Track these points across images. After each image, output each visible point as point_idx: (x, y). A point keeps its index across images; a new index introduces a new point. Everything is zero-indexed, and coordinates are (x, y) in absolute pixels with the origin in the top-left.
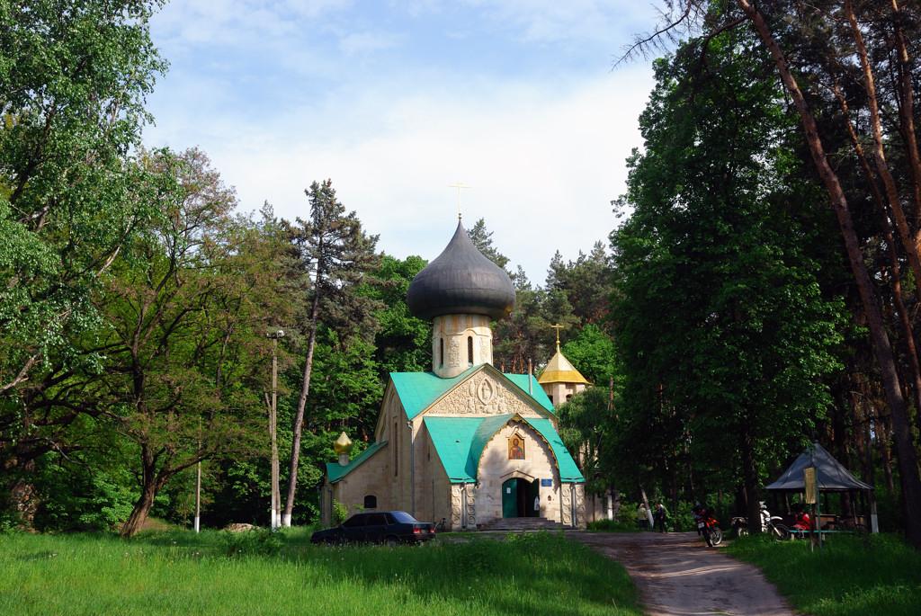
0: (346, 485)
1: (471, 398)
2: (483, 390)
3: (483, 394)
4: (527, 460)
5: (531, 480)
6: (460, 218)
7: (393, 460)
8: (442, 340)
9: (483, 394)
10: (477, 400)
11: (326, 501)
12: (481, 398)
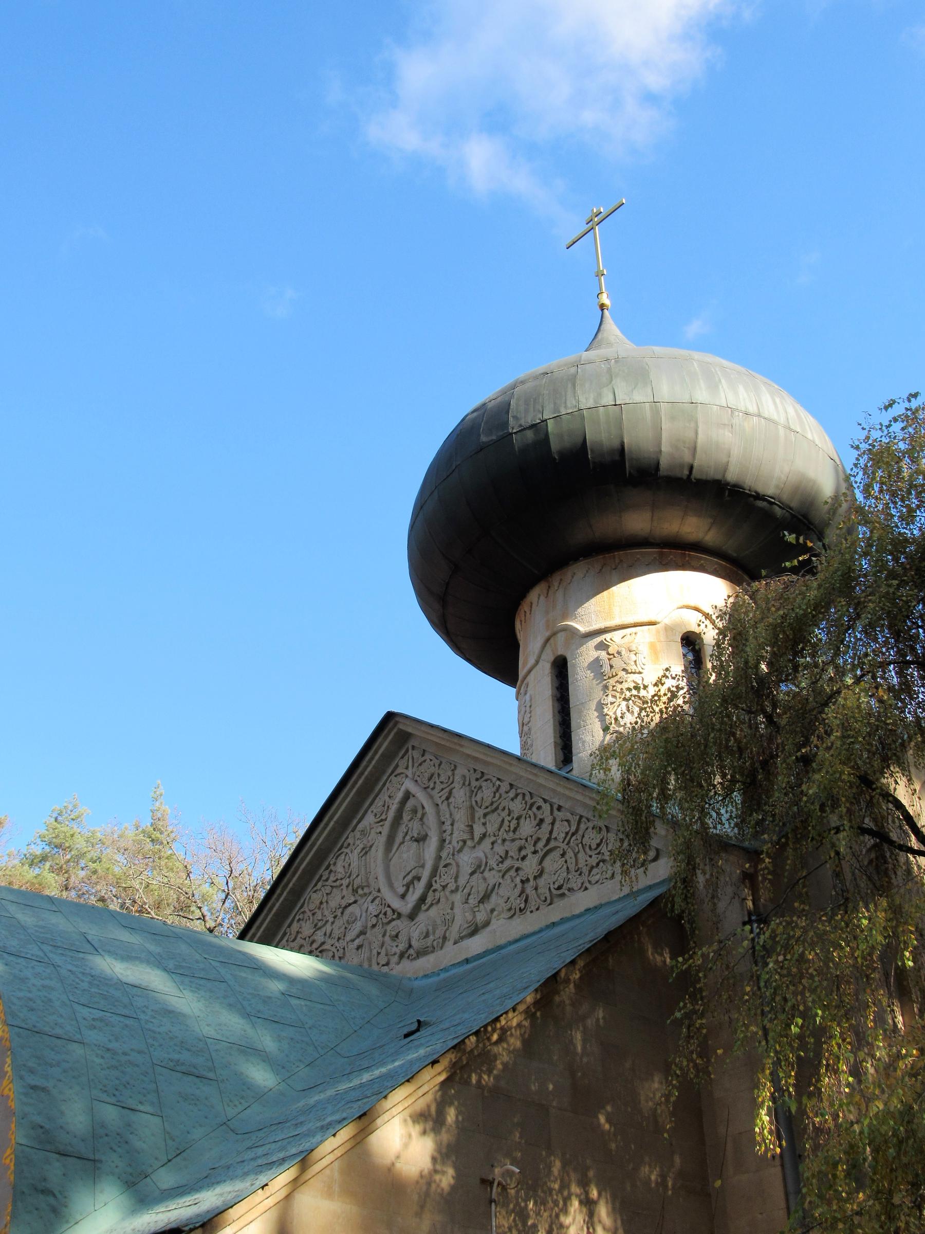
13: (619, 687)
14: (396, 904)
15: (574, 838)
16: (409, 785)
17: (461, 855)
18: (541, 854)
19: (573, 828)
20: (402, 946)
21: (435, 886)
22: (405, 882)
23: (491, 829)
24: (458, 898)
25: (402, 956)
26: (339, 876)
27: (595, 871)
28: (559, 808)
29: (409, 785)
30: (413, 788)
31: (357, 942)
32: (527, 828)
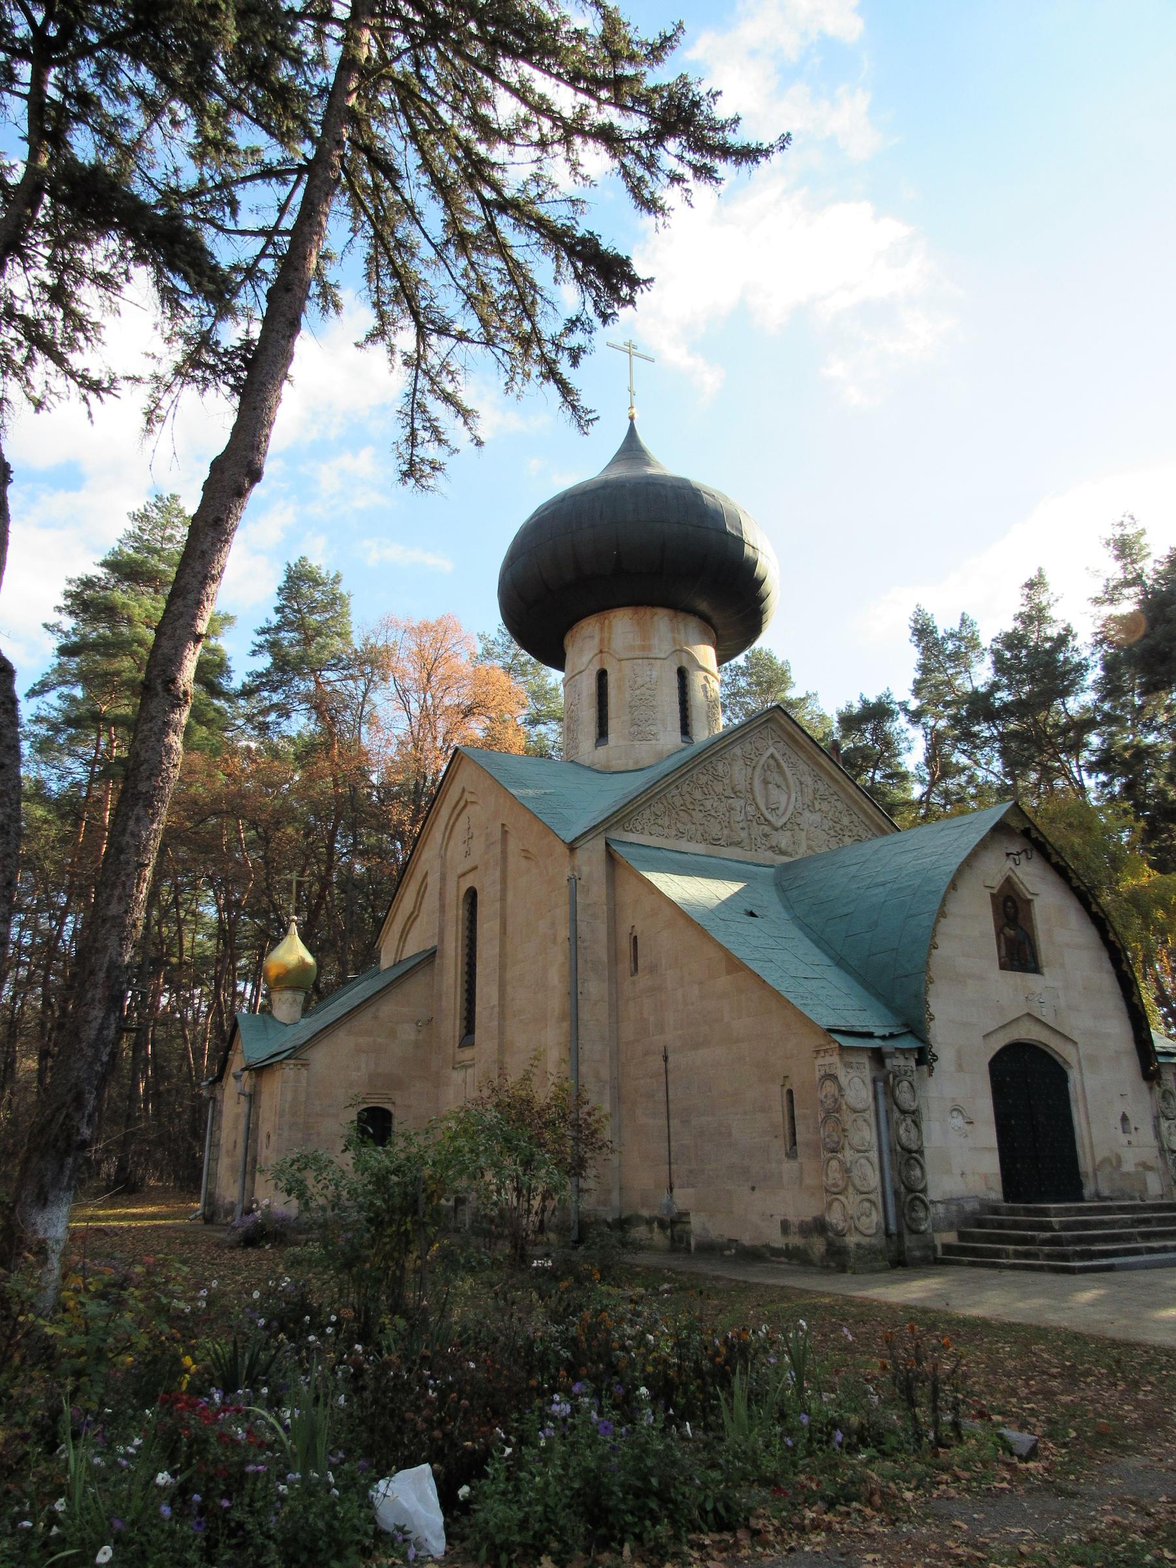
0: (304, 1072)
1: (738, 804)
2: (766, 782)
3: (767, 797)
7: (453, 1001)
8: (602, 675)
9: (767, 797)
10: (751, 809)
11: (227, 1121)
12: (763, 808)
14: (769, 817)
16: (772, 750)
29: (772, 750)
30: (777, 756)
32: (845, 821)
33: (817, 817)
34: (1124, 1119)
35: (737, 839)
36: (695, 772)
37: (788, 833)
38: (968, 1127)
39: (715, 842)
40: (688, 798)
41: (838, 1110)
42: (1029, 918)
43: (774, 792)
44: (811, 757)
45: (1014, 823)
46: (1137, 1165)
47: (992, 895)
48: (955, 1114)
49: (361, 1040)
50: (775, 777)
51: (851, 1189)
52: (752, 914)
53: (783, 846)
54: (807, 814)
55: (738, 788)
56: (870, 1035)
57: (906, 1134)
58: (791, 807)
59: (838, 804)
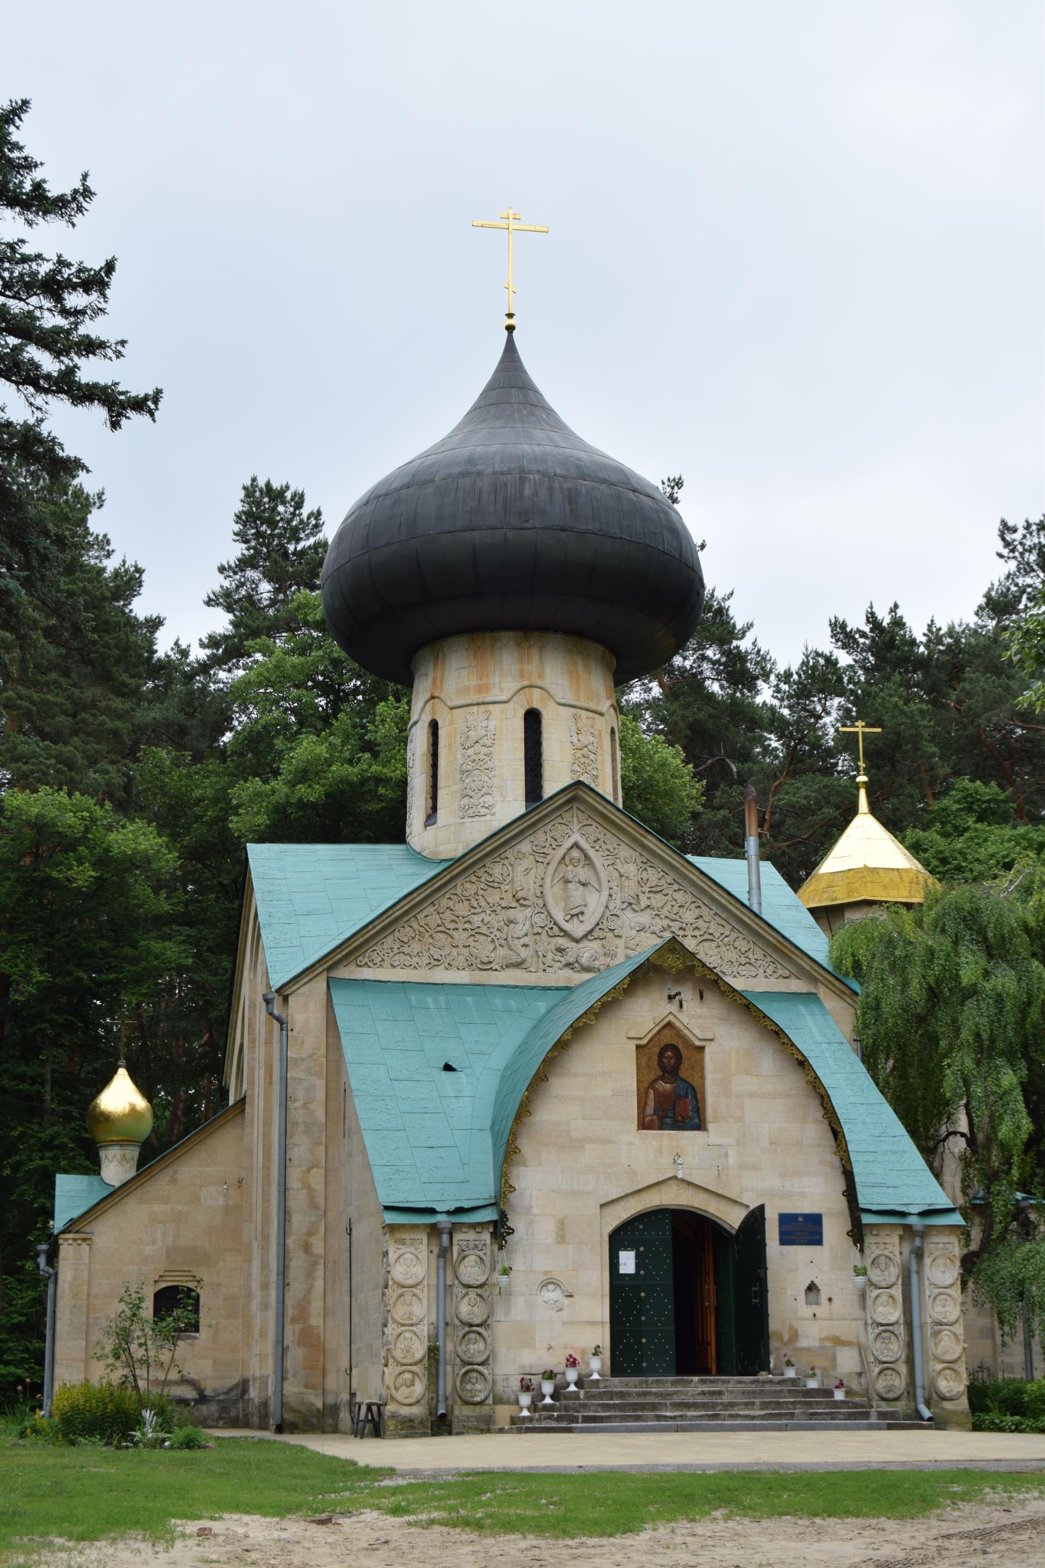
0: (85, 1247)
1: (520, 915)
3: (567, 898)
4: (714, 1133)
5: (733, 1219)
6: (510, 329)
8: (434, 726)
9: (567, 898)
10: (540, 920)
12: (559, 916)
13: (583, 760)
14: (566, 926)
15: (726, 940)
17: (625, 912)
18: (700, 939)
19: (727, 933)
20: (571, 960)
21: (601, 926)
22: (573, 912)
23: (654, 904)
24: (620, 942)
25: (568, 965)
26: (496, 880)
27: (741, 968)
28: (716, 914)
29: (576, 837)
31: (522, 941)
32: (689, 916)
33: (645, 918)
34: (812, 1288)
35: (515, 959)
36: (460, 881)
37: (595, 945)
38: (567, 1301)
39: (486, 966)
40: (448, 916)
41: (386, 1287)
42: (699, 1067)
43: (576, 892)
44: (636, 840)
45: (672, 962)
46: (821, 1339)
47: (638, 1047)
48: (551, 1287)
49: (156, 1208)
50: (583, 873)
51: (391, 1361)
52: (448, 1068)
53: (584, 961)
54: (629, 913)
55: (520, 895)
56: (432, 1211)
57: (467, 1308)
58: (602, 909)
59: (680, 896)
